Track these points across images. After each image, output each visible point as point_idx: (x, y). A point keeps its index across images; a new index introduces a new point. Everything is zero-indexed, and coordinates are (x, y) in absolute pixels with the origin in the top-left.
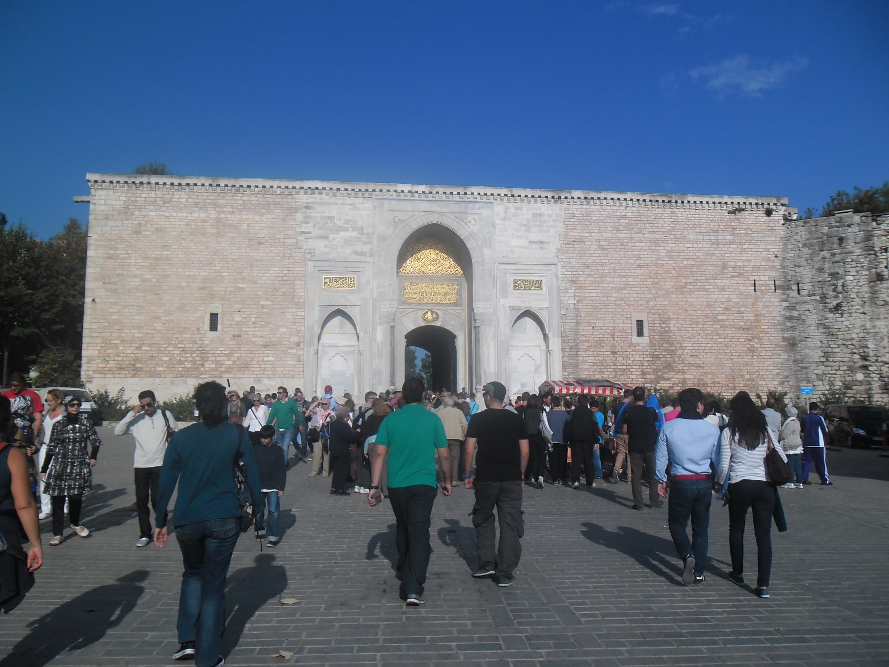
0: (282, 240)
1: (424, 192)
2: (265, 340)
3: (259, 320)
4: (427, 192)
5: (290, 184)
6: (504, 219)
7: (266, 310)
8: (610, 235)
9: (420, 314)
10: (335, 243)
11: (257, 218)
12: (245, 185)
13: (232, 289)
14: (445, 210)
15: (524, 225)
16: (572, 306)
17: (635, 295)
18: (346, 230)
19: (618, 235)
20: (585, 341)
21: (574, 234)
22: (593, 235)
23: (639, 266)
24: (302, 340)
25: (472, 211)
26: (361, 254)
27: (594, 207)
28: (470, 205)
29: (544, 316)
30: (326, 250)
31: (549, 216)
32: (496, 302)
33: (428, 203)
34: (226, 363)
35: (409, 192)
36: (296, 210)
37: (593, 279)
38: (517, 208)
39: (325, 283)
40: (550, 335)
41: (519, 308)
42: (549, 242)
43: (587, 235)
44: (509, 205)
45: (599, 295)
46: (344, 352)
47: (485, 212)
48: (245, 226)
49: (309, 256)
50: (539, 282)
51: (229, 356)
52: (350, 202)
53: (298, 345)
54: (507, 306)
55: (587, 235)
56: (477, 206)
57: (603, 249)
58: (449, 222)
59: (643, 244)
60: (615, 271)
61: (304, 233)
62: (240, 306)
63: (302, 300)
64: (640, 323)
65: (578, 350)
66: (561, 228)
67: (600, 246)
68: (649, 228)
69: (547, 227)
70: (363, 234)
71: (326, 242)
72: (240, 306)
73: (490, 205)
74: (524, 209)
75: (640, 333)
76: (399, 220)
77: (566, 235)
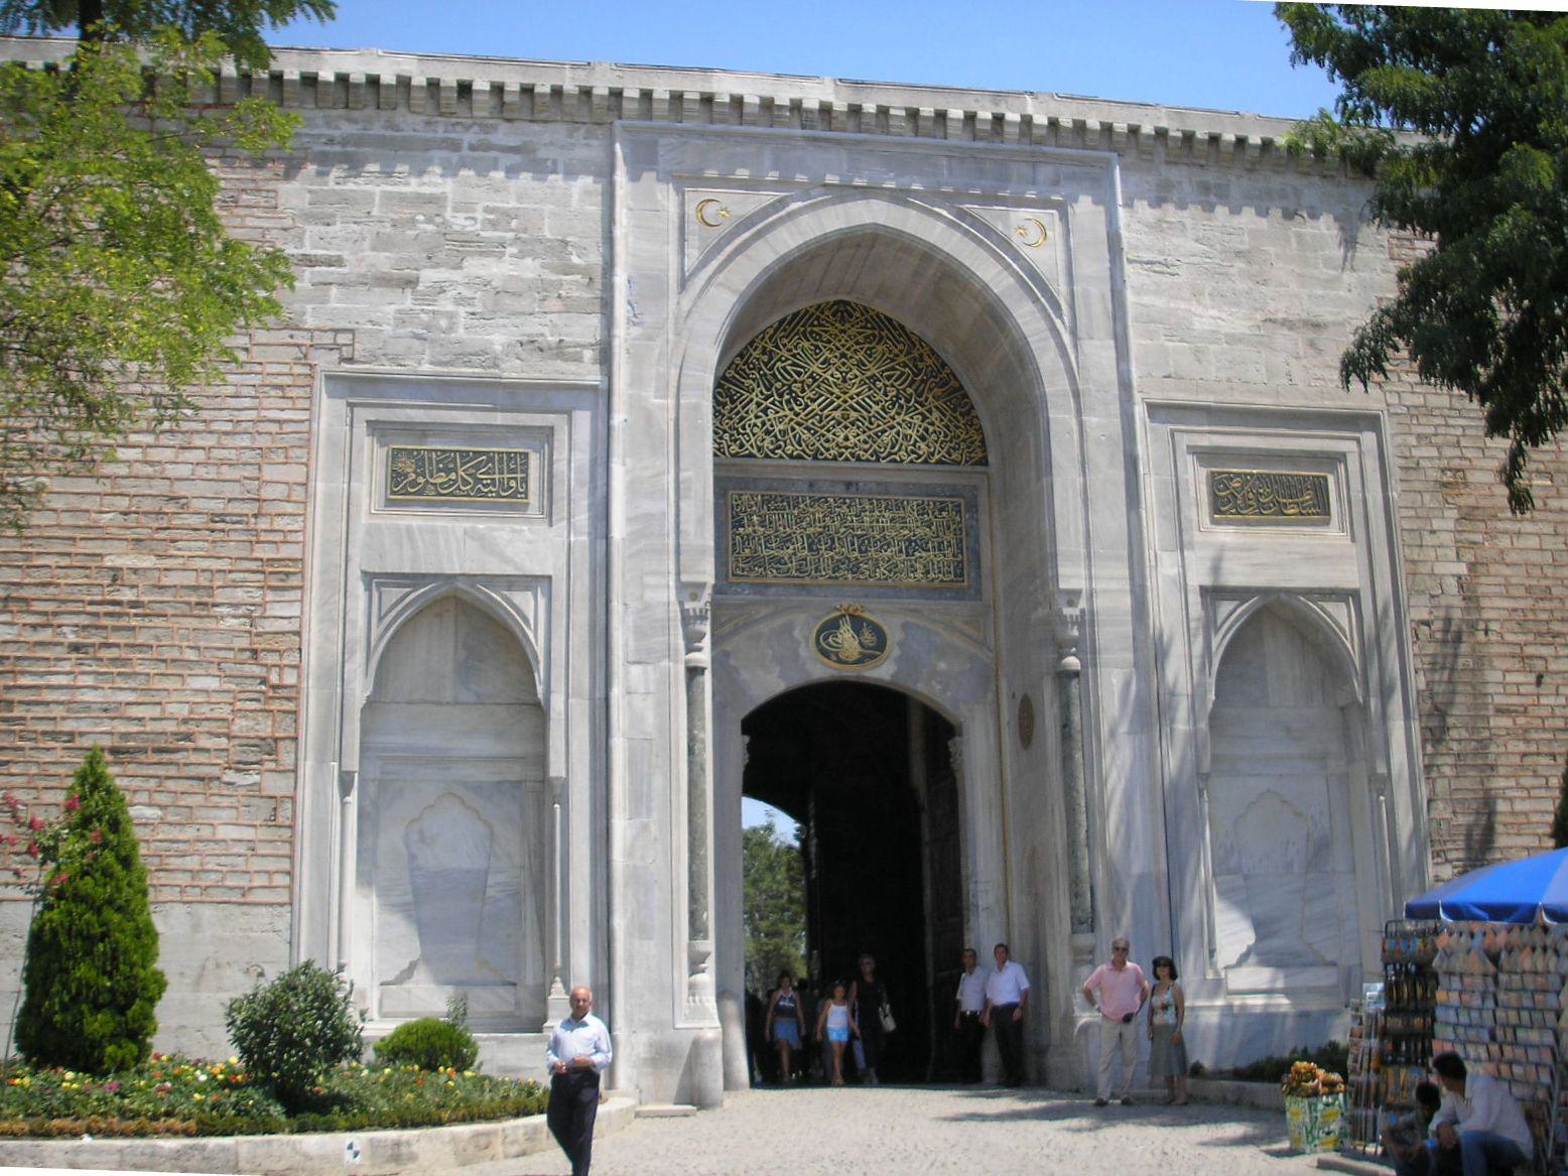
9: (804, 628)
10: (445, 304)
15: (1238, 254)
16: (1452, 585)
18: (496, 249)
24: (285, 729)
26: (560, 351)
39: (396, 478)
45: (1549, 543)
46: (477, 788)
52: (513, 142)
63: (287, 551)
70: (569, 269)
71: (407, 301)
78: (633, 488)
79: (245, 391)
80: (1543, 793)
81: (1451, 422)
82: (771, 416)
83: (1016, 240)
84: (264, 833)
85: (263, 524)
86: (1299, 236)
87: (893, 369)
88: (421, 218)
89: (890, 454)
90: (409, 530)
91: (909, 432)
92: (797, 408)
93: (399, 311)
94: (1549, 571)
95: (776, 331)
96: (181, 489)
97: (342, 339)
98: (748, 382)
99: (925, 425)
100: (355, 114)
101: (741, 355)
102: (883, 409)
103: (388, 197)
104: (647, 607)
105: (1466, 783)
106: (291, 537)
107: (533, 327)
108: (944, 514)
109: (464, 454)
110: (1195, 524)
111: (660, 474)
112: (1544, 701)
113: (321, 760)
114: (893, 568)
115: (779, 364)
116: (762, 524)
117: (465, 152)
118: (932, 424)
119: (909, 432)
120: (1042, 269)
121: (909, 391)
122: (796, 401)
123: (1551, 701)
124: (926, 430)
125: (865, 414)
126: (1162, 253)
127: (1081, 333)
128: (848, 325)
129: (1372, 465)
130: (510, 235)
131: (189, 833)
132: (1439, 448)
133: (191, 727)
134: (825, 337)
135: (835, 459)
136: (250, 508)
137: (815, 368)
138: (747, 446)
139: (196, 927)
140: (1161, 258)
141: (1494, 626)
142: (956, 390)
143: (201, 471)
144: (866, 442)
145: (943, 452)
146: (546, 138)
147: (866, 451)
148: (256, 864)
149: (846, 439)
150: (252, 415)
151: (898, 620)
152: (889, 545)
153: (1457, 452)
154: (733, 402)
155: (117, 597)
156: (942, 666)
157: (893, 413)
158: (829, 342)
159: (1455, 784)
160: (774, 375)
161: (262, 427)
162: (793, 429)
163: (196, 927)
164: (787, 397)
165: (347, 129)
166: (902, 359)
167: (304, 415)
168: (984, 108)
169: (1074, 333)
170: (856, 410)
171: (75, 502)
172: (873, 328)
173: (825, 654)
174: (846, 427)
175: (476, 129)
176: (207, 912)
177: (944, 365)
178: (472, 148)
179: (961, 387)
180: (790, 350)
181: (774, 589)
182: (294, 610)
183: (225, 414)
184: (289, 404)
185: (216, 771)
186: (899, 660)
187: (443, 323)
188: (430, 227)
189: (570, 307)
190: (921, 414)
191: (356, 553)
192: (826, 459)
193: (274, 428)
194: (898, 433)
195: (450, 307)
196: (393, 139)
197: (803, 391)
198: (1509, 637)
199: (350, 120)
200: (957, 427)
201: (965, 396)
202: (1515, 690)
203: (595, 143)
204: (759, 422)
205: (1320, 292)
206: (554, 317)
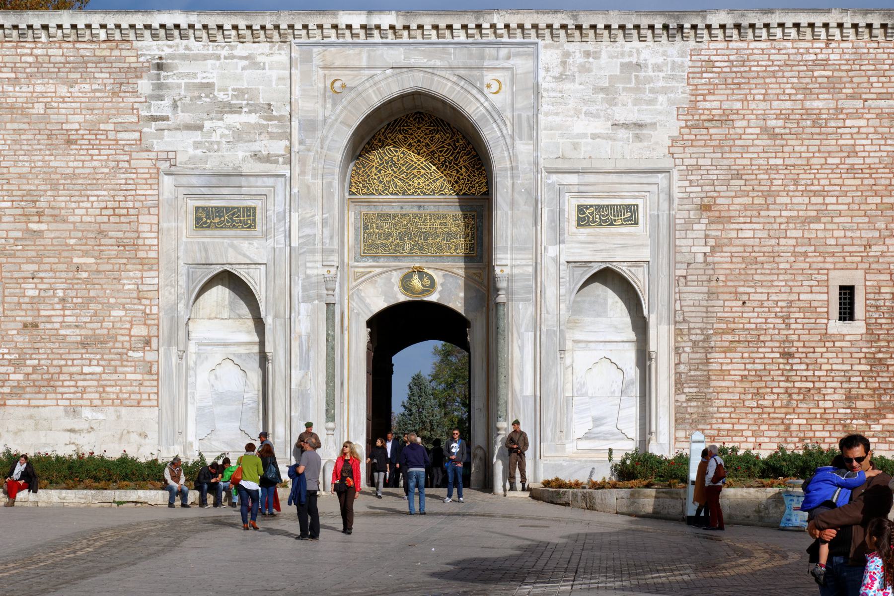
0: (111, 135)
1: (392, 27)
2: (83, 332)
3: (72, 293)
4: (399, 26)
5: (125, 21)
6: (560, 78)
7: (84, 275)
8: (788, 104)
10: (215, 137)
11: (63, 90)
12: (37, 24)
13: (19, 234)
14: (438, 63)
15: (602, 89)
17: (837, 234)
18: (238, 110)
19: (808, 104)
20: (725, 332)
21: (711, 104)
22: (753, 105)
23: (851, 169)
24: (154, 331)
25: (495, 63)
26: (268, 159)
27: (756, 46)
28: (488, 51)
29: (639, 279)
30: (199, 152)
31: (658, 68)
32: (538, 253)
33: (401, 49)
34: (12, 377)
35: (363, 27)
36: (137, 72)
37: (748, 200)
38: (587, 54)
39: (198, 219)
40: (652, 321)
41: (587, 264)
42: (653, 125)
43: (738, 105)
44: (570, 47)
45: (759, 234)
47: (522, 65)
48: (39, 108)
49: (164, 166)
50: (632, 209)
51: (17, 364)
52: (245, 54)
53: (148, 342)
54: (563, 259)
55: (738, 105)
56: (504, 51)
57: (774, 136)
58: (446, 88)
59: (863, 123)
60: (796, 184)
61: (154, 119)
62: (35, 267)
63: (153, 255)
64: (847, 293)
65: (708, 350)
66: (682, 93)
67: (765, 129)
68: (877, 88)
69: (652, 91)
70: (271, 118)
71: (197, 136)
72: (35, 267)
73: (531, 49)
74: (604, 55)
75: (847, 313)
76: (344, 86)
77: (693, 107)
78: (302, 224)
79: (129, 182)
80: (739, 361)
81: (710, 172)
83: (486, 90)
84: (147, 377)
85: (140, 242)
86: (637, 77)
87: (443, 147)
88: (203, 95)
90: (203, 243)
93: (195, 142)
94: (756, 249)
96: (103, 227)
97: (171, 155)
100: (170, 43)
103: (187, 85)
104: (308, 277)
105: (698, 356)
106: (153, 248)
107: (256, 147)
109: (227, 208)
110: (566, 232)
111: (314, 215)
112: (745, 315)
113: (170, 345)
117: (222, 60)
120: (498, 106)
123: (751, 315)
126: (561, 92)
127: (516, 138)
129: (663, 196)
130: (245, 102)
131: (115, 377)
132: (701, 186)
133: (114, 332)
136: (135, 235)
139: (119, 417)
140: (560, 95)
141: (722, 278)
143: (112, 219)
146: (260, 51)
148: (143, 389)
150: (133, 192)
153: (712, 188)
155: (79, 276)
158: (412, 134)
159: (691, 356)
161: (137, 198)
163: (119, 417)
165: (167, 51)
167: (156, 192)
168: (471, 22)
169: (512, 137)
171: (57, 234)
175: (227, 48)
176: (124, 411)
178: (225, 58)
182: (155, 281)
183: (121, 193)
184: (149, 187)
185: (125, 351)
187: (216, 147)
188: (208, 100)
189: (272, 136)
191: (181, 254)
193: (143, 198)
195: (218, 139)
196: (189, 55)
198: (730, 283)
199: (170, 47)
202: (729, 309)
203: (283, 52)
205: (645, 107)
206: (265, 142)
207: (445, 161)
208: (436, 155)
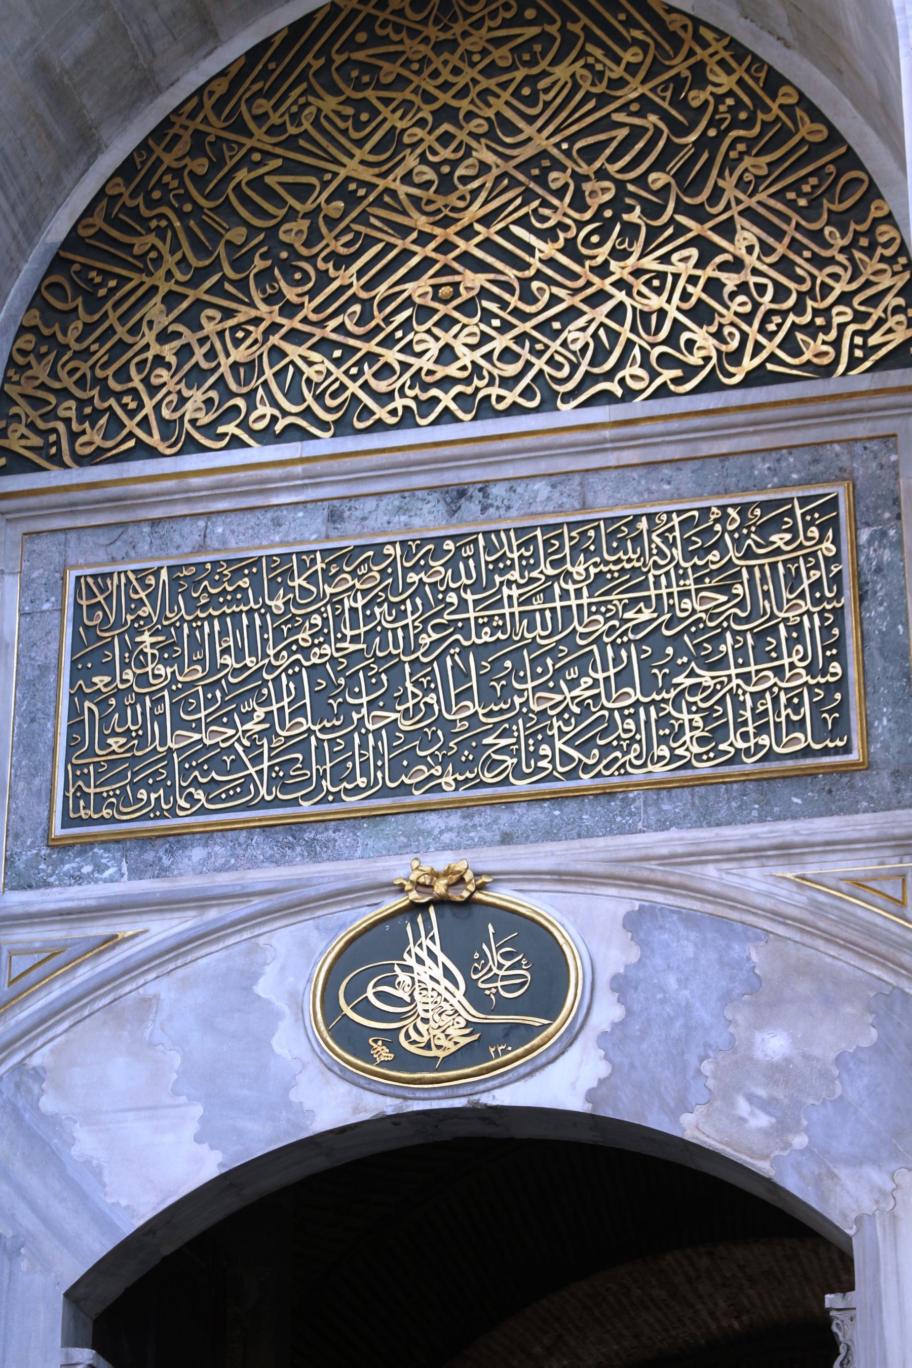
9: (292, 961)
82: (210, 328)
87: (606, 124)
89: (590, 379)
91: (655, 302)
92: (291, 294)
95: (236, 83)
98: (141, 243)
99: (710, 271)
101: (126, 170)
102: (569, 249)
108: (779, 539)
114: (595, 733)
115: (243, 175)
116: (167, 652)
118: (736, 265)
119: (655, 302)
121: (658, 179)
122: (288, 269)
124: (713, 287)
125: (511, 274)
128: (458, 28)
134: (389, 71)
135: (407, 420)
137: (352, 168)
138: (131, 425)
142: (816, 150)
144: (508, 355)
145: (771, 346)
147: (508, 383)
149: (447, 354)
151: (613, 904)
152: (584, 662)
154: (93, 303)
156: (774, 1044)
157: (603, 253)
158: (401, 82)
160: (225, 207)
162: (277, 353)
164: (259, 264)
166: (631, 93)
170: (480, 267)
172: (543, 18)
173: (351, 1038)
174: (446, 322)
177: (775, 81)
179: (835, 137)
180: (272, 130)
181: (197, 853)
186: (611, 1041)
190: (698, 241)
192: (380, 426)
194: (617, 313)
197: (313, 237)
200: (819, 262)
201: (850, 160)
204: (168, 352)
207: (618, 204)
208: (556, 179)
